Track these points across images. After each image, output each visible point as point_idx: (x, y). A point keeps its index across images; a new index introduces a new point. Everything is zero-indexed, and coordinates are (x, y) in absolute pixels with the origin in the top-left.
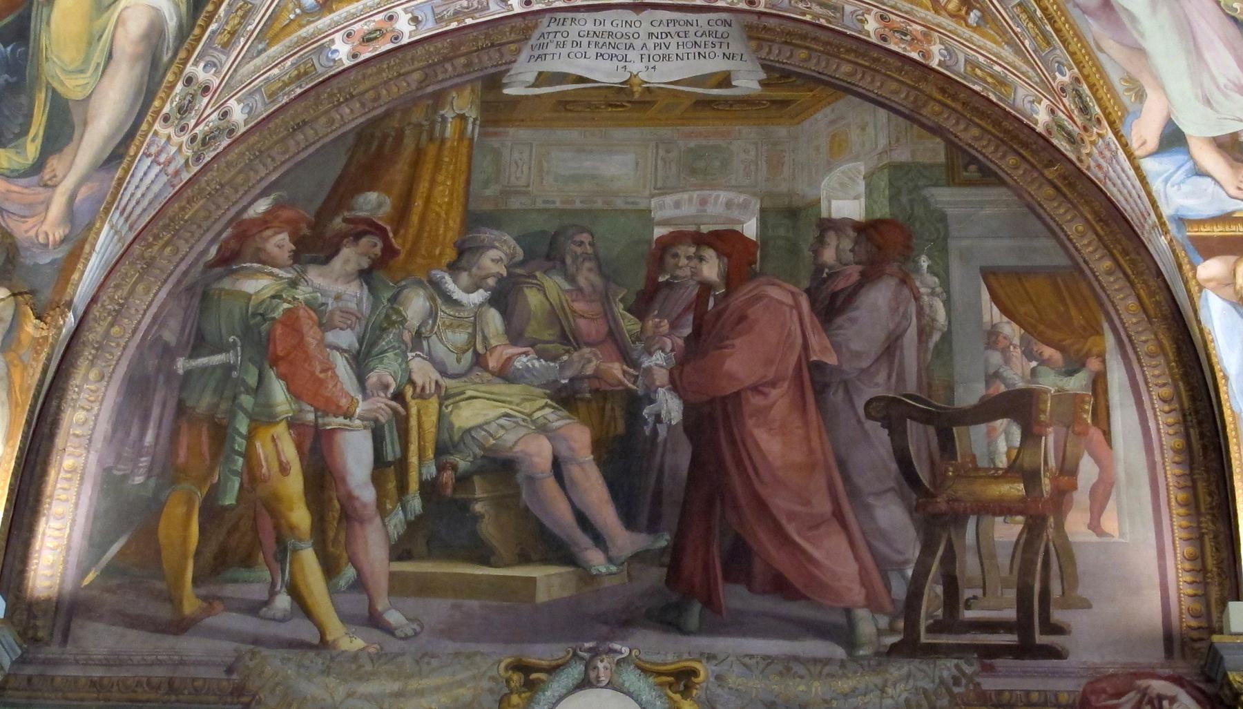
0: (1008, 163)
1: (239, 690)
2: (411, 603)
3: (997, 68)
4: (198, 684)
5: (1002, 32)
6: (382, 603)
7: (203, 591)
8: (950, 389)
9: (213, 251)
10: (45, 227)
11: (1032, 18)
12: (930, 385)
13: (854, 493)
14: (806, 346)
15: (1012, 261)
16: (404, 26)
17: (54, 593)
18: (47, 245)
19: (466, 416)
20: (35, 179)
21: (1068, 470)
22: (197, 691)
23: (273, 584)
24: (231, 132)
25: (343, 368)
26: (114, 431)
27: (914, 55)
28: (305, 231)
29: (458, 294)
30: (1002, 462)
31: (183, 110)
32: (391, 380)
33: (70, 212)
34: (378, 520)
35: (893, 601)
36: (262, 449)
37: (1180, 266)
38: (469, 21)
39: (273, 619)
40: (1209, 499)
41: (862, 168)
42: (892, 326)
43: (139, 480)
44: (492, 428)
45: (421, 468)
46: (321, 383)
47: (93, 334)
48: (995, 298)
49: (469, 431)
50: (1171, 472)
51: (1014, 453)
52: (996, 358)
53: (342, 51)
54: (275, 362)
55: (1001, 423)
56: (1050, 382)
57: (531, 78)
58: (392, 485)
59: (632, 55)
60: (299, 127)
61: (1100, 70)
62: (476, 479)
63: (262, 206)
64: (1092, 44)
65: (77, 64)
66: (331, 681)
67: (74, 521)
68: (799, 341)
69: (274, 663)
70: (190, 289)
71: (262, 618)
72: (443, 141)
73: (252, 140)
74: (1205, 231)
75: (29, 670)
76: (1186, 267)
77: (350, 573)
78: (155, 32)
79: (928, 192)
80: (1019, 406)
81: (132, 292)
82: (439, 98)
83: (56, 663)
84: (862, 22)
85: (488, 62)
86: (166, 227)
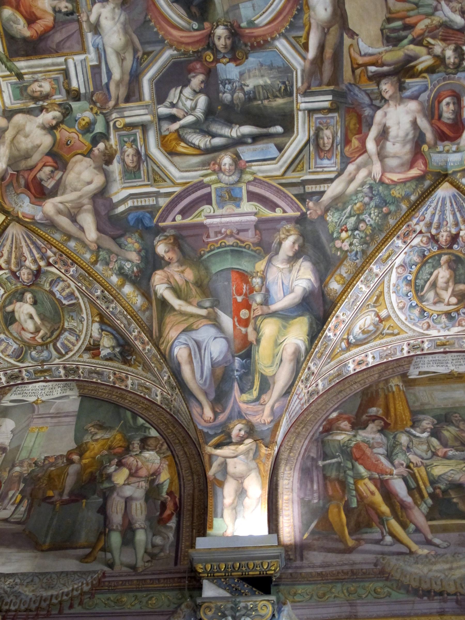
1: (382, 572)
2: (442, 535)
4: (364, 571)
6: (430, 536)
7: (354, 537)
9: (321, 429)
10: (263, 418)
16: (370, 359)
17: (292, 542)
18: (265, 424)
19: (437, 471)
20: (257, 403)
22: (364, 573)
23: (382, 533)
24: (318, 393)
25: (384, 460)
26: (301, 485)
28: (353, 420)
29: (418, 434)
31: (307, 379)
32: (403, 462)
33: (272, 412)
34: (416, 508)
36: (361, 487)
38: (390, 359)
39: (386, 545)
43: (316, 501)
44: (449, 474)
45: (427, 490)
46: (377, 465)
47: (284, 455)
49: (440, 476)
53: (351, 367)
54: (357, 460)
57: (417, 373)
58: (417, 496)
60: (341, 391)
62: (450, 491)
63: (334, 415)
65: (269, 364)
66: (420, 566)
67: (293, 517)
69: (393, 560)
70: (317, 440)
71: (382, 545)
72: (393, 392)
73: (325, 396)
75: (290, 571)
77: (412, 527)
78: (297, 352)
81: (294, 442)
82: (387, 381)
83: (301, 567)
85: (400, 370)
86: (301, 423)
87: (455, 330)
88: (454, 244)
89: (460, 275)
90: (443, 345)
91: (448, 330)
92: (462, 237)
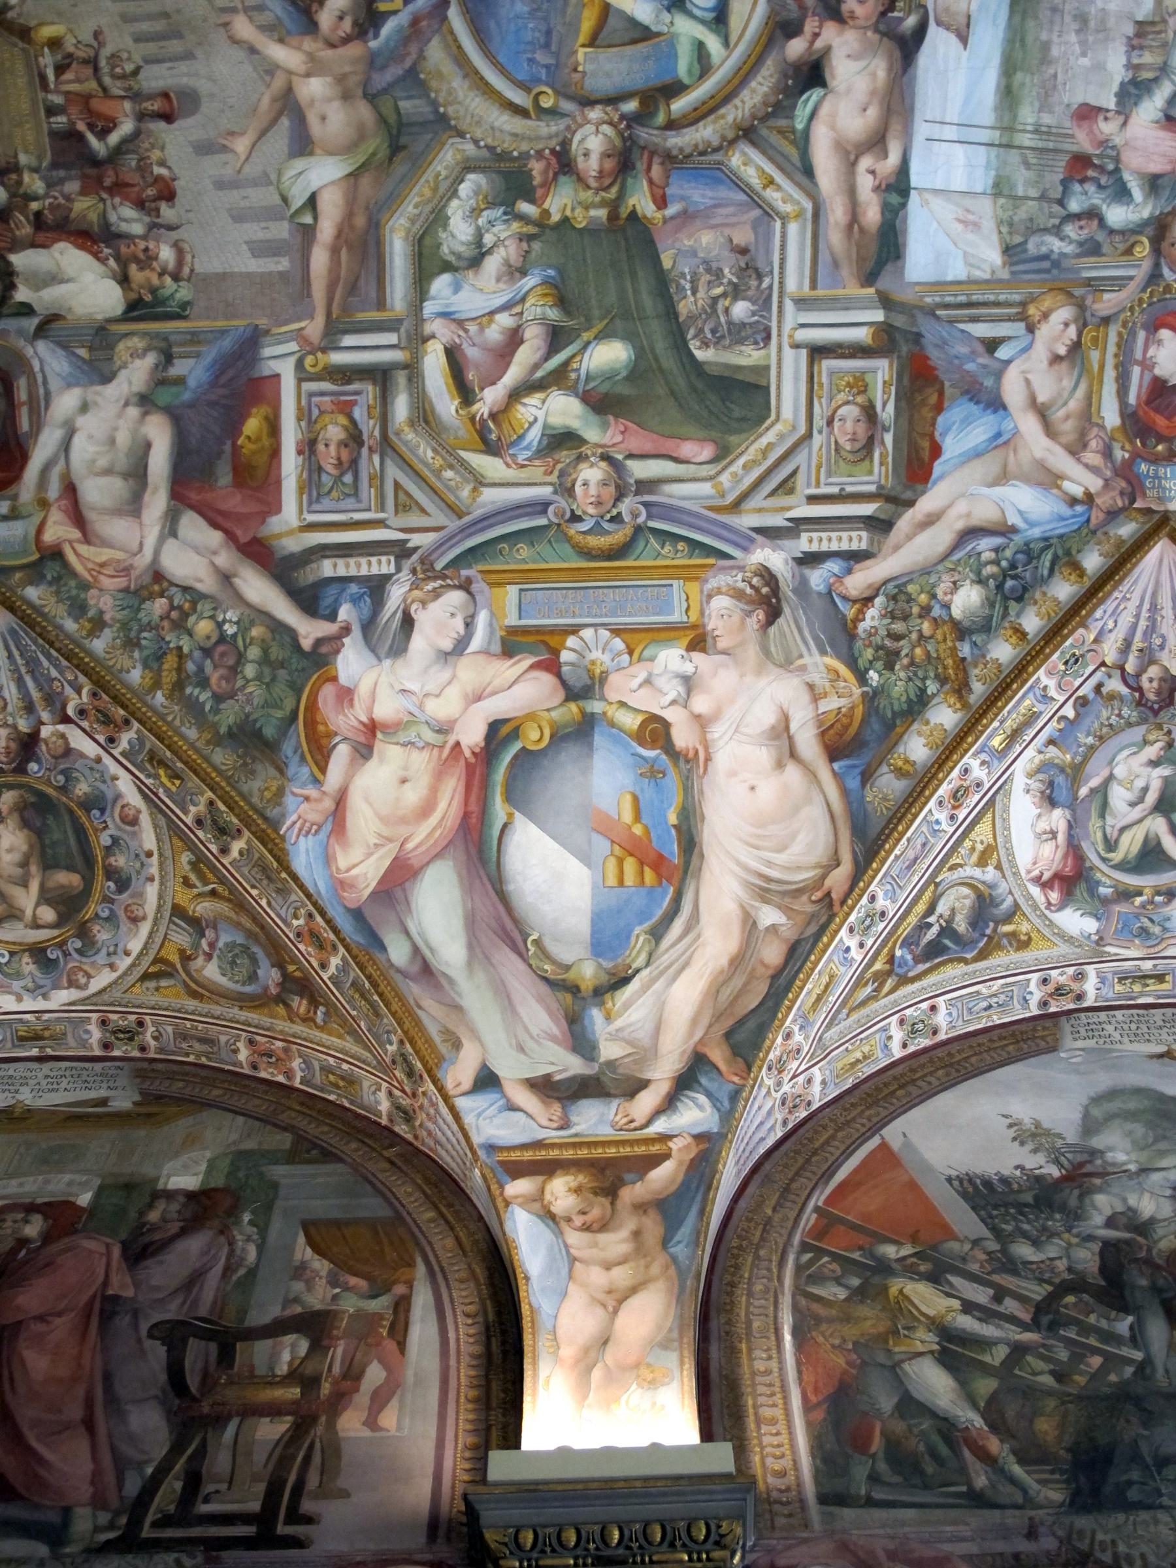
0: (351, 1148)
3: (345, 1066)
5: (344, 1023)
8: (243, 1312)
11: (363, 996)
12: (222, 1309)
13: (112, 1401)
14: (106, 1283)
15: (336, 1214)
21: (353, 1375)
27: (281, 1078)
30: (283, 1369)
35: (122, 1498)
37: (489, 1189)
40: (502, 1395)
41: (208, 1154)
42: (198, 1265)
48: (311, 1242)
50: (464, 1374)
51: (298, 1362)
52: (298, 1287)
55: (289, 1338)
56: (350, 1305)
59: (24, 1089)
61: (418, 1023)
64: (412, 1002)
68: (101, 1278)
74: (515, 1156)
76: (494, 1187)
79: (264, 1169)
80: (315, 1326)
84: (236, 1051)
87: (62, 997)
88: (28, 761)
89: (54, 844)
90: (37, 1037)
91: (45, 996)
92: (46, 742)
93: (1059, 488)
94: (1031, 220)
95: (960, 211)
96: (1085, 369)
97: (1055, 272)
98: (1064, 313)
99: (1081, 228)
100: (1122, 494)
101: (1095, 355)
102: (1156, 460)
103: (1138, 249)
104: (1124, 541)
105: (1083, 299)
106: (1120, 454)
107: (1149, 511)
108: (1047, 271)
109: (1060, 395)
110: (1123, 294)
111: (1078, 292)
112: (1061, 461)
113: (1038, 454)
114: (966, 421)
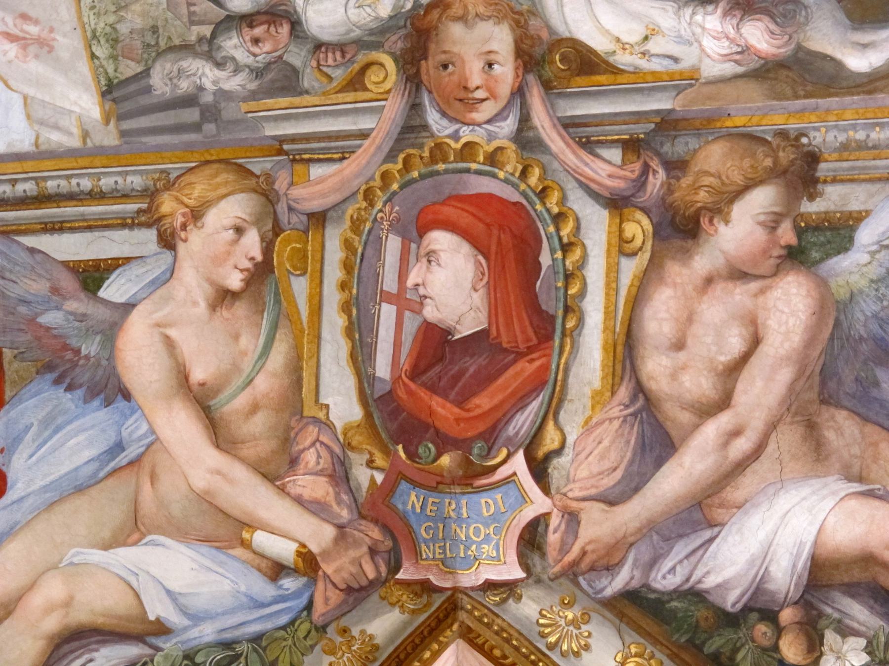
93: (246, 545)
94: (154, 30)
95: (9, 20)
96: (283, 315)
97: (210, 128)
98: (234, 208)
99: (256, 41)
100: (373, 552)
101: (300, 287)
102: (438, 484)
103: (373, 77)
104: (376, 648)
105: (269, 178)
106: (364, 476)
107: (425, 588)
108: (196, 127)
109: (236, 368)
110: (350, 166)
111: (258, 165)
112: (250, 494)
113: (200, 480)
114: (52, 425)
